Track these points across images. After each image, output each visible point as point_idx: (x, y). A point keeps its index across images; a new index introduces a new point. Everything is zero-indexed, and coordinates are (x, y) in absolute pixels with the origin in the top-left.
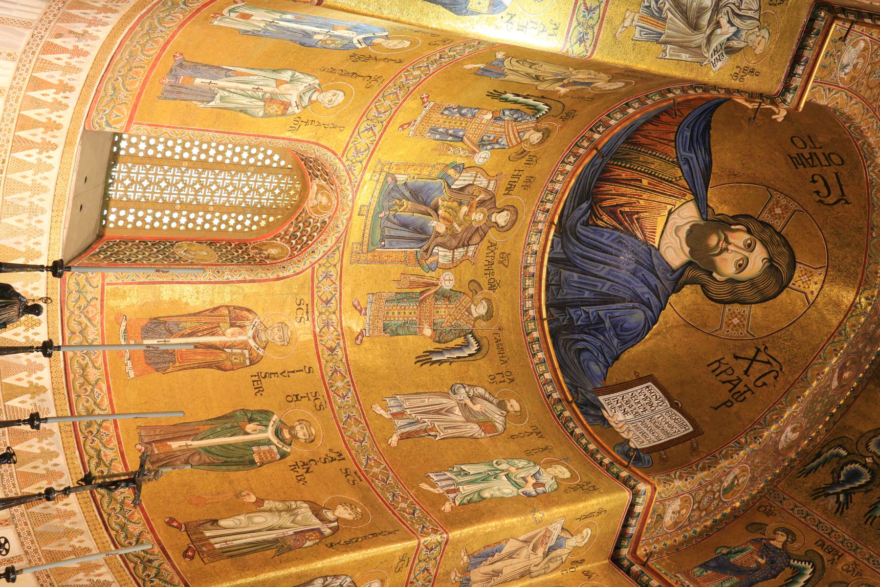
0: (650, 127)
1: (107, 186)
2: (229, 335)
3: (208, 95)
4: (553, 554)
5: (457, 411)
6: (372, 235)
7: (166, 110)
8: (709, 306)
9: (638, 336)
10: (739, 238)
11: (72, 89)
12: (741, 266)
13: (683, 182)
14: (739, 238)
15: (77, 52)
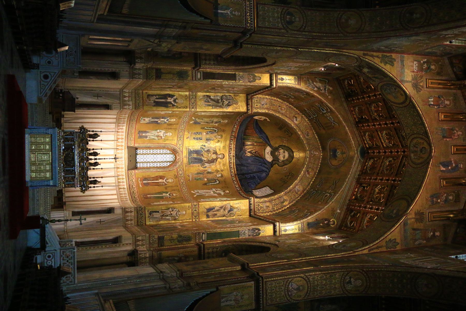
0: (247, 131)
1: (136, 159)
2: (160, 181)
3: (146, 137)
4: (230, 213)
5: (212, 192)
6: (189, 162)
7: (140, 140)
8: (279, 168)
9: (265, 178)
10: (282, 151)
11: (123, 139)
12: (284, 157)
13: (264, 142)
14: (282, 151)
15: (122, 132)
